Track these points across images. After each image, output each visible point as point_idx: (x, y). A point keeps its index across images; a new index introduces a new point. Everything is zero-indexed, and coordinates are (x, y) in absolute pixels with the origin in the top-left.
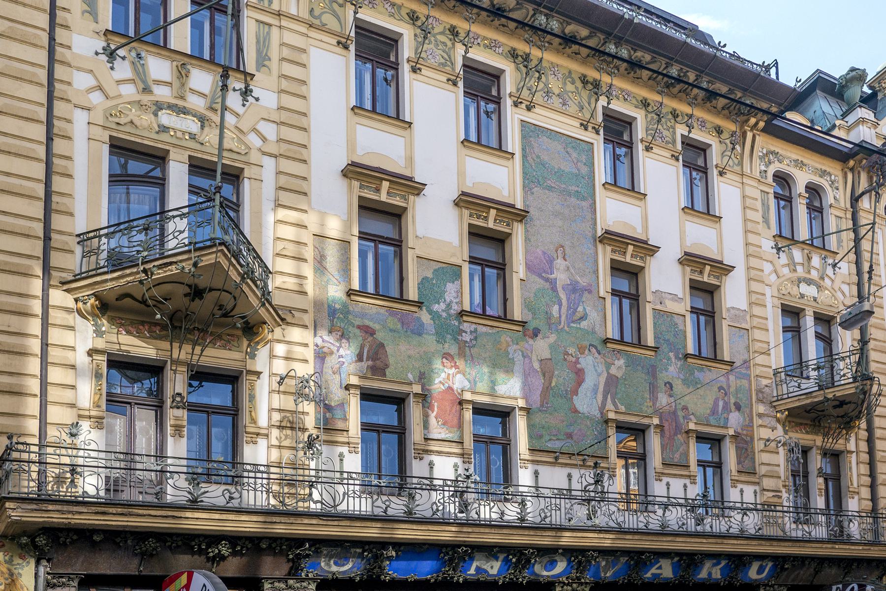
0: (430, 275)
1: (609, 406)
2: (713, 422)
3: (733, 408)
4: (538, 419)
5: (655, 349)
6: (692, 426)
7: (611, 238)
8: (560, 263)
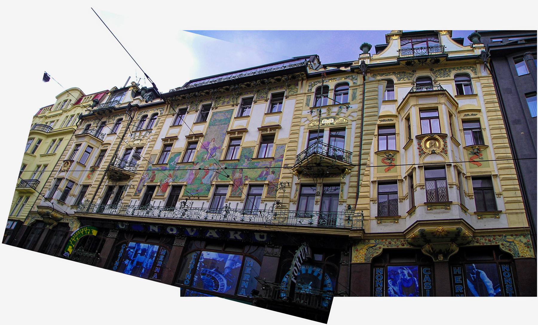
0: (173, 156)
1: (215, 179)
2: (258, 179)
3: (271, 173)
4: (189, 187)
5: (238, 160)
6: (247, 182)
7: (232, 132)
8: (212, 143)
